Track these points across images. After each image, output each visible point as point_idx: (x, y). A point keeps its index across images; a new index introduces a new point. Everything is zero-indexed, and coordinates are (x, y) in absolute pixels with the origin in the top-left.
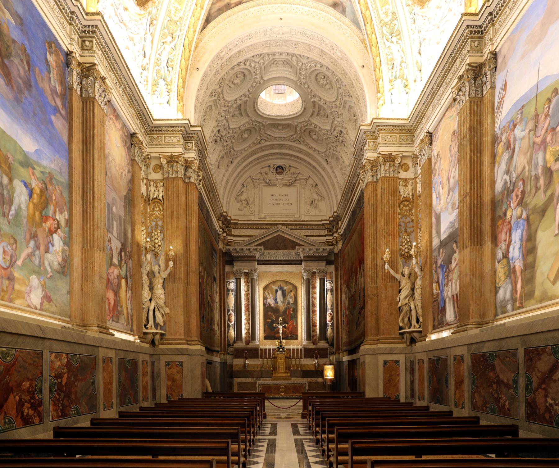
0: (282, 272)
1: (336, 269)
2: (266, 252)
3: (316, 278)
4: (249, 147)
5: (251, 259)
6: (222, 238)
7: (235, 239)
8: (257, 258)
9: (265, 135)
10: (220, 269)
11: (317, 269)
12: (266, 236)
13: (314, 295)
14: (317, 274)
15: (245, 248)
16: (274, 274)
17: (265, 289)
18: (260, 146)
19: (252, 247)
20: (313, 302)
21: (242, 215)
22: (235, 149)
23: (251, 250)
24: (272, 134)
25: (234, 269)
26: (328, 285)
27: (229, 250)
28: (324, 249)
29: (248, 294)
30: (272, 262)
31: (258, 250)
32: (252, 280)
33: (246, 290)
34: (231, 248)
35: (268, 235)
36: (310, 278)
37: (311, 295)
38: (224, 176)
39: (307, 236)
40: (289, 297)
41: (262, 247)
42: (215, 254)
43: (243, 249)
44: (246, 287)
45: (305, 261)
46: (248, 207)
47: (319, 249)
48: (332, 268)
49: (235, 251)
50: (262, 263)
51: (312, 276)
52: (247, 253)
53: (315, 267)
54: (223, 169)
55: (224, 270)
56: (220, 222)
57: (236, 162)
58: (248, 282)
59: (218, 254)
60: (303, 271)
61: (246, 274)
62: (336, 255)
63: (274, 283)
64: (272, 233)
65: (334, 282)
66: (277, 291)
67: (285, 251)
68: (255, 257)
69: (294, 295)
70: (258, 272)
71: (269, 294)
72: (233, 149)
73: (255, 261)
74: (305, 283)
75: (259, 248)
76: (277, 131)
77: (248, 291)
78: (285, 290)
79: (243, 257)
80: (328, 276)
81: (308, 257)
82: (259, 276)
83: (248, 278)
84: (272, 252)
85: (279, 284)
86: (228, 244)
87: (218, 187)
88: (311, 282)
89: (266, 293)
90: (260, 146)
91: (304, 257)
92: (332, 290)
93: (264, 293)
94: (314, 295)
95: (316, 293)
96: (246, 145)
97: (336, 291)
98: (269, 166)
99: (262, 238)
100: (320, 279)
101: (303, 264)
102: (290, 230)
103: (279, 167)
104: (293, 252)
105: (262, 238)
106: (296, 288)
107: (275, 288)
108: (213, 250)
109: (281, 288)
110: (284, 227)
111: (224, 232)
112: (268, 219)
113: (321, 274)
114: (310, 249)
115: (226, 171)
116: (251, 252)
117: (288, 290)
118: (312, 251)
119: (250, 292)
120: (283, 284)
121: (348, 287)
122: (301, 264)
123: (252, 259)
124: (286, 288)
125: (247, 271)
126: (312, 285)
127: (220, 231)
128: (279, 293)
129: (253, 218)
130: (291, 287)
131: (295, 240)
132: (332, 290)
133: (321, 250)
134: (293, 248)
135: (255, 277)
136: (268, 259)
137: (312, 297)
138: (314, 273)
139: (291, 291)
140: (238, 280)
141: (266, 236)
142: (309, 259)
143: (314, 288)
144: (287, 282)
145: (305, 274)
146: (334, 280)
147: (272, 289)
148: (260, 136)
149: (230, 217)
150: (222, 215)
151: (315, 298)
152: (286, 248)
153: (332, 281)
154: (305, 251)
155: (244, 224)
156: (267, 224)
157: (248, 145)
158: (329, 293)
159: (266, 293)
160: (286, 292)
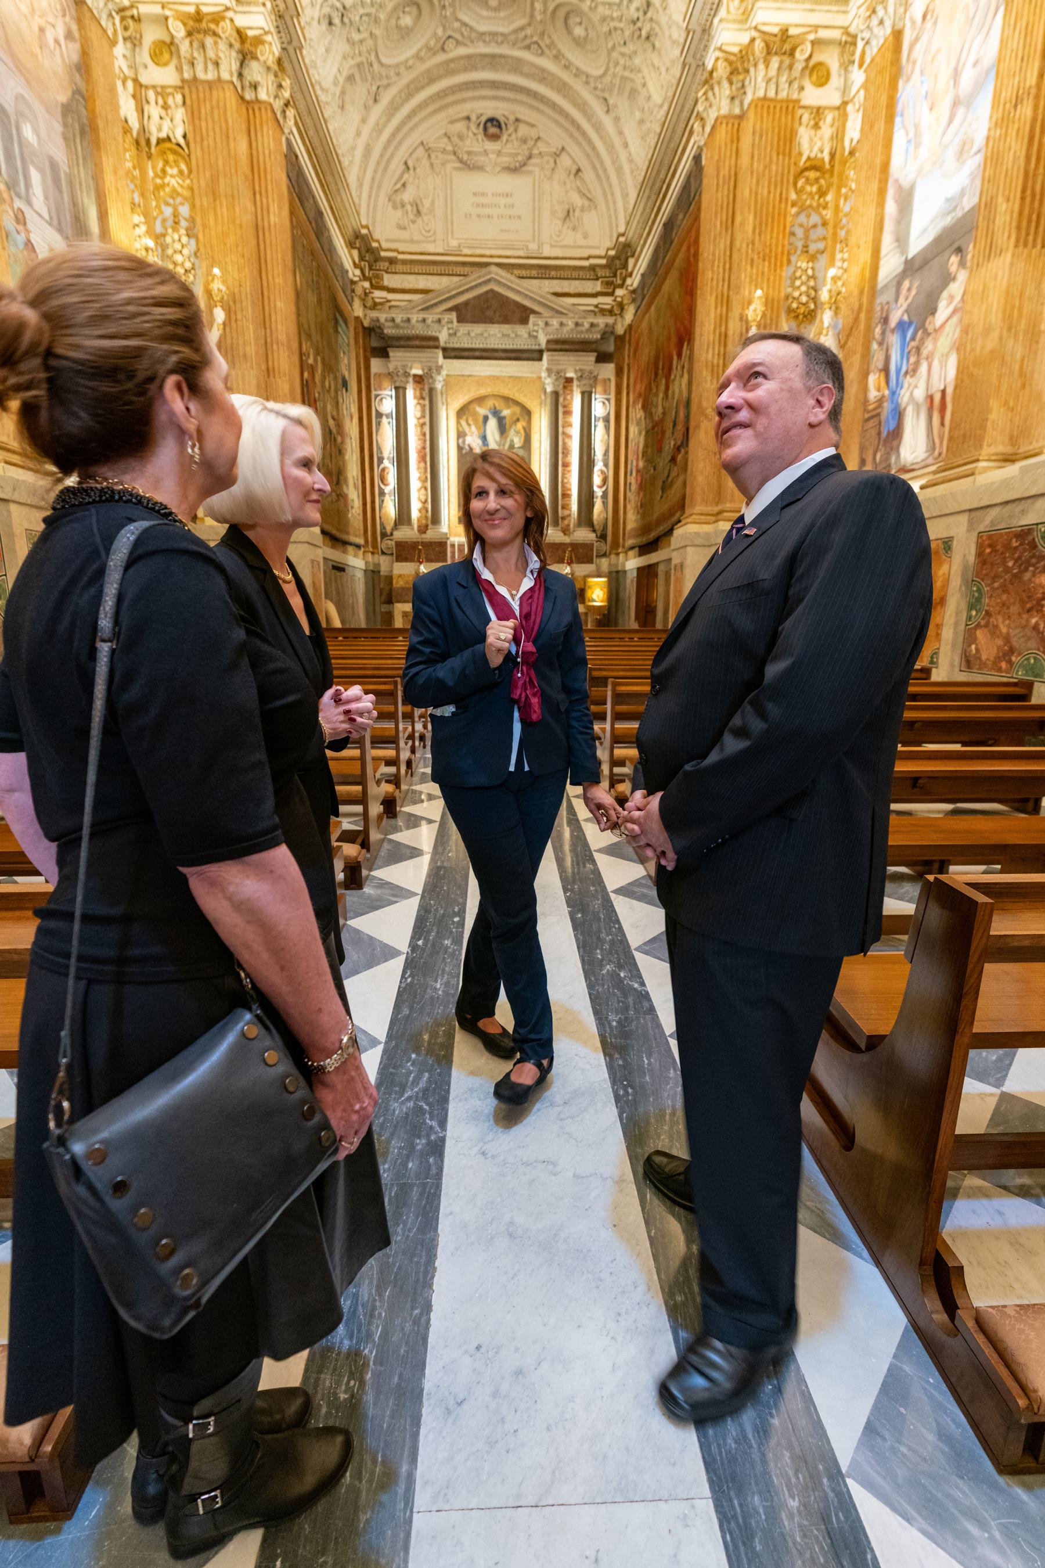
0: (498, 378)
1: (619, 372)
2: (464, 329)
3: (572, 391)
4: (417, 56)
5: (428, 342)
6: (359, 290)
7: (390, 296)
8: (442, 343)
9: (456, 25)
10: (358, 364)
11: (576, 371)
12: (462, 293)
13: (568, 430)
14: (575, 382)
15: (415, 318)
16: (481, 381)
17: (461, 412)
18: (442, 57)
19: (430, 317)
20: (564, 444)
21: (404, 241)
22: (384, 60)
23: (429, 321)
24: (472, 23)
25: (392, 366)
26: (599, 408)
27: (378, 320)
28: (592, 325)
29: (423, 425)
30: (477, 354)
31: (444, 322)
32: (431, 391)
33: (419, 414)
34: (383, 317)
35: (467, 290)
36: (560, 389)
37: (560, 430)
38: (358, 134)
39: (556, 294)
40: (512, 432)
41: (453, 316)
42: (343, 325)
43: (408, 320)
44: (419, 407)
45: (549, 350)
46: (419, 220)
47: (582, 325)
48: (608, 370)
49: (390, 324)
50: (453, 354)
51: (565, 387)
52: (420, 330)
53: (572, 365)
54: (354, 115)
55: (368, 368)
56: (355, 253)
57: (386, 98)
58: (423, 398)
59: (352, 329)
60: (544, 375)
61: (419, 380)
62: (620, 340)
63: (480, 400)
64: (476, 286)
65: (613, 402)
66: (486, 419)
67: (506, 328)
68: (436, 339)
69: (524, 428)
70: (444, 373)
71: (469, 425)
72: (377, 56)
73: (437, 347)
74: (548, 401)
75: (446, 317)
76: (485, 13)
77: (423, 417)
78: (504, 418)
79: (409, 338)
80: (599, 389)
81: (557, 342)
82: (447, 383)
83: (422, 389)
84: (477, 329)
85: (490, 403)
86: (375, 306)
87: (345, 162)
88: (561, 399)
89: (463, 423)
90: (442, 57)
91: (548, 342)
92: (606, 420)
93: (458, 423)
94: (568, 430)
95: (571, 425)
96: (408, 52)
97: (618, 420)
98: (468, 118)
99: (453, 297)
100: (583, 393)
101: (545, 356)
102: (517, 281)
103: (491, 120)
104: (522, 331)
105: (453, 297)
106: (528, 413)
107: (482, 411)
108: (337, 314)
109: (496, 413)
110: (503, 272)
111: (365, 278)
112: (466, 251)
113: (583, 382)
114: (562, 324)
115: (364, 121)
116: (428, 326)
117: (511, 413)
118: (565, 329)
119: (427, 420)
120: (499, 404)
121: (644, 407)
122: (540, 359)
123: (431, 343)
124: (506, 412)
125: (419, 372)
126: (564, 407)
127: (354, 273)
128: (492, 424)
129: (431, 248)
130: (518, 410)
131: (527, 303)
132: (606, 420)
133: (587, 325)
134: (524, 321)
135: (439, 386)
136: (466, 346)
137: (564, 433)
138: (569, 380)
139: (518, 420)
140: (401, 391)
141: (462, 293)
142: (559, 347)
143: (568, 413)
144: (508, 400)
145: (548, 381)
146: (612, 396)
147: (475, 414)
148: (444, 27)
149: (378, 241)
150: (357, 236)
151: (570, 437)
152: (506, 320)
153: (608, 400)
154: (549, 329)
155: (412, 262)
156: (464, 264)
157: (413, 51)
158: (601, 425)
159: (463, 423)
160: (507, 421)
